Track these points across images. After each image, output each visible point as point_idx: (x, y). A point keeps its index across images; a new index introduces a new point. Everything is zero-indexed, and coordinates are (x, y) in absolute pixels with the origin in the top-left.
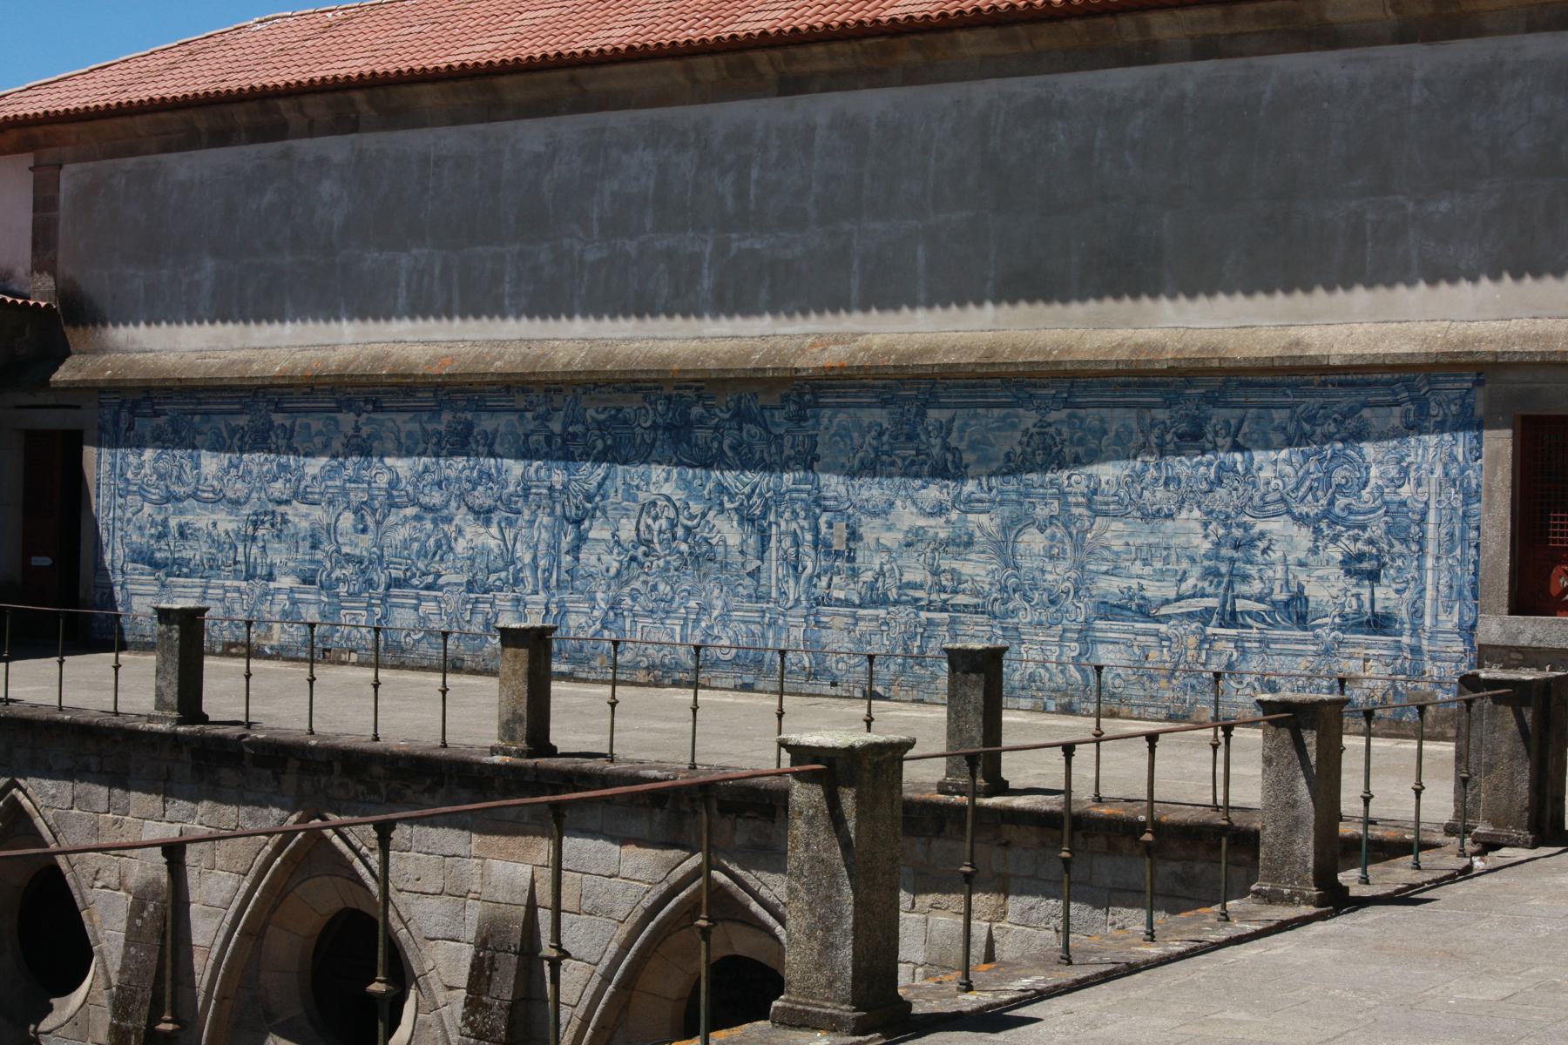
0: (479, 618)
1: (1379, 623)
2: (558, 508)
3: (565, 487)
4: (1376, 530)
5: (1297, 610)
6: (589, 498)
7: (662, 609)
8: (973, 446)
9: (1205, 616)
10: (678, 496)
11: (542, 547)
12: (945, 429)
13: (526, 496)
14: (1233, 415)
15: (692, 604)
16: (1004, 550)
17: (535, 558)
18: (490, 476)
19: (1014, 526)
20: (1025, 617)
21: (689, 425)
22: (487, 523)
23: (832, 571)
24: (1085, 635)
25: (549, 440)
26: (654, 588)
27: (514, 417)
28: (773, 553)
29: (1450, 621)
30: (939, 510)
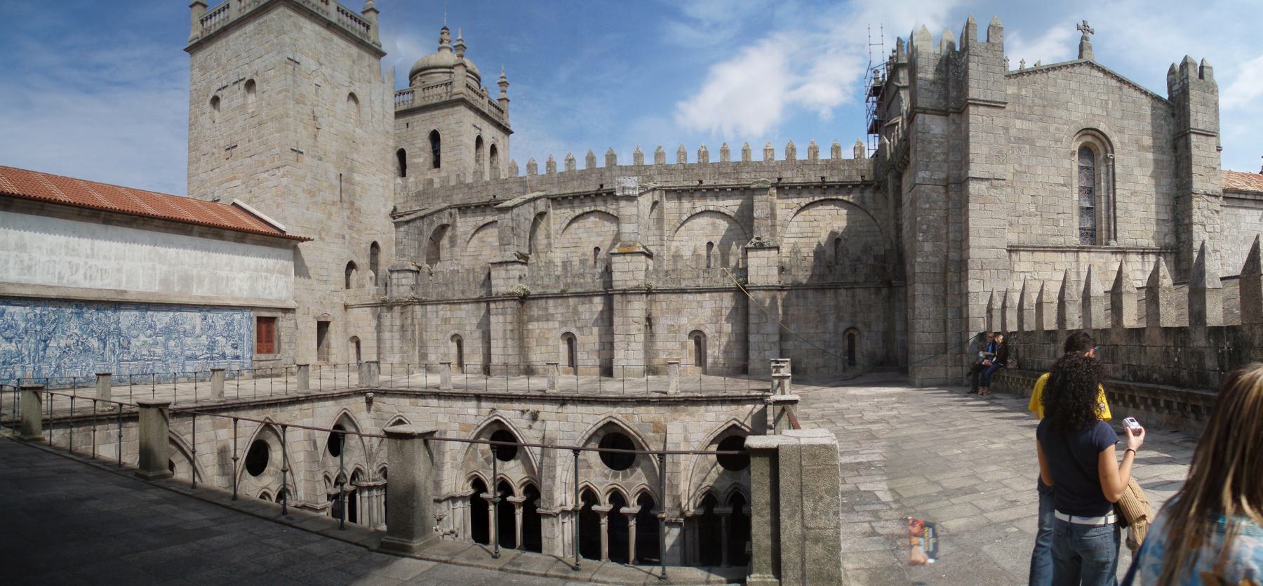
0: (8, 374)
1: (238, 357)
2: (38, 338)
3: (41, 331)
4: (236, 339)
5: (224, 356)
6: (49, 334)
7: (74, 366)
8: (158, 320)
9: (207, 358)
10: (79, 333)
11: (32, 349)
12: (152, 316)
13: (26, 334)
14: (212, 315)
15: (84, 364)
16: (166, 348)
17: (29, 353)
18: (12, 327)
19: (167, 340)
20: (170, 361)
21: (83, 313)
22: (11, 342)
23: (123, 353)
24: (183, 365)
25: (35, 315)
26: (72, 360)
27: (22, 308)
28: (107, 348)
29: (248, 356)
30: (150, 336)
